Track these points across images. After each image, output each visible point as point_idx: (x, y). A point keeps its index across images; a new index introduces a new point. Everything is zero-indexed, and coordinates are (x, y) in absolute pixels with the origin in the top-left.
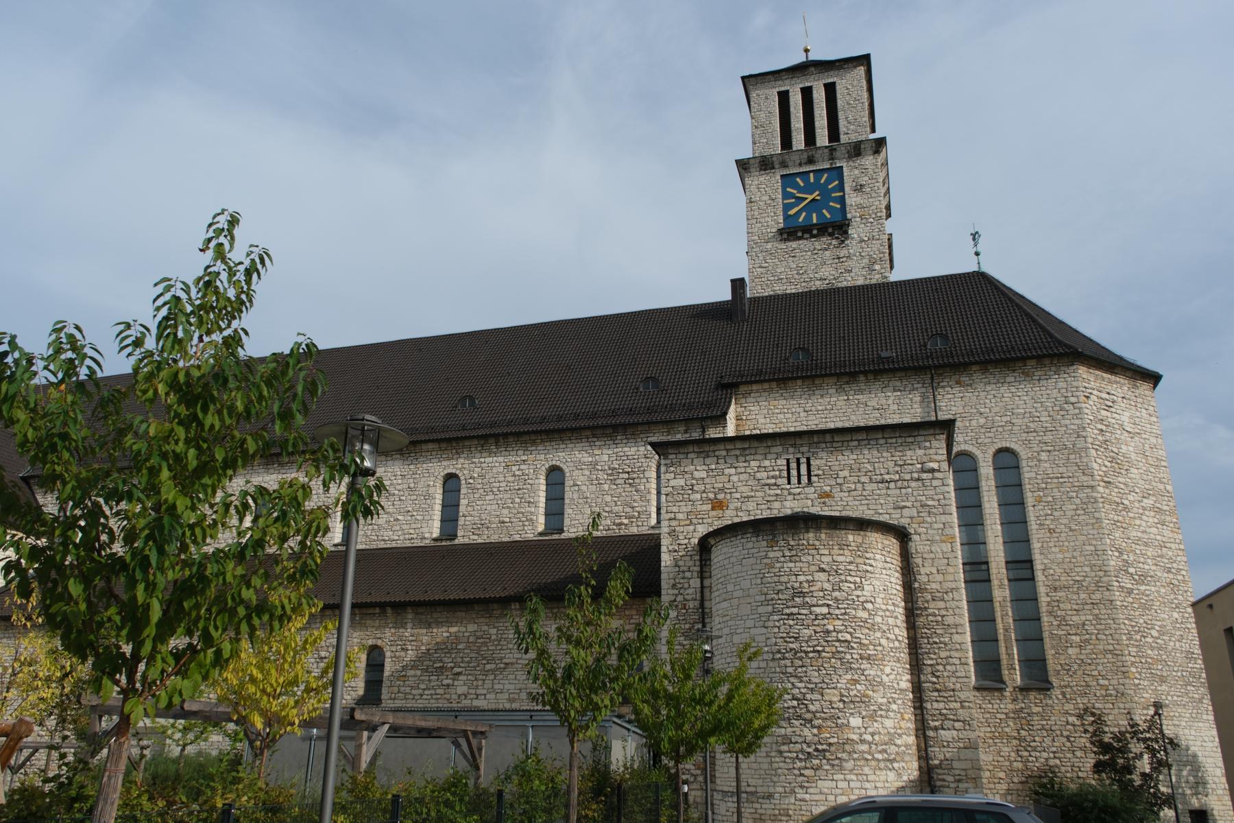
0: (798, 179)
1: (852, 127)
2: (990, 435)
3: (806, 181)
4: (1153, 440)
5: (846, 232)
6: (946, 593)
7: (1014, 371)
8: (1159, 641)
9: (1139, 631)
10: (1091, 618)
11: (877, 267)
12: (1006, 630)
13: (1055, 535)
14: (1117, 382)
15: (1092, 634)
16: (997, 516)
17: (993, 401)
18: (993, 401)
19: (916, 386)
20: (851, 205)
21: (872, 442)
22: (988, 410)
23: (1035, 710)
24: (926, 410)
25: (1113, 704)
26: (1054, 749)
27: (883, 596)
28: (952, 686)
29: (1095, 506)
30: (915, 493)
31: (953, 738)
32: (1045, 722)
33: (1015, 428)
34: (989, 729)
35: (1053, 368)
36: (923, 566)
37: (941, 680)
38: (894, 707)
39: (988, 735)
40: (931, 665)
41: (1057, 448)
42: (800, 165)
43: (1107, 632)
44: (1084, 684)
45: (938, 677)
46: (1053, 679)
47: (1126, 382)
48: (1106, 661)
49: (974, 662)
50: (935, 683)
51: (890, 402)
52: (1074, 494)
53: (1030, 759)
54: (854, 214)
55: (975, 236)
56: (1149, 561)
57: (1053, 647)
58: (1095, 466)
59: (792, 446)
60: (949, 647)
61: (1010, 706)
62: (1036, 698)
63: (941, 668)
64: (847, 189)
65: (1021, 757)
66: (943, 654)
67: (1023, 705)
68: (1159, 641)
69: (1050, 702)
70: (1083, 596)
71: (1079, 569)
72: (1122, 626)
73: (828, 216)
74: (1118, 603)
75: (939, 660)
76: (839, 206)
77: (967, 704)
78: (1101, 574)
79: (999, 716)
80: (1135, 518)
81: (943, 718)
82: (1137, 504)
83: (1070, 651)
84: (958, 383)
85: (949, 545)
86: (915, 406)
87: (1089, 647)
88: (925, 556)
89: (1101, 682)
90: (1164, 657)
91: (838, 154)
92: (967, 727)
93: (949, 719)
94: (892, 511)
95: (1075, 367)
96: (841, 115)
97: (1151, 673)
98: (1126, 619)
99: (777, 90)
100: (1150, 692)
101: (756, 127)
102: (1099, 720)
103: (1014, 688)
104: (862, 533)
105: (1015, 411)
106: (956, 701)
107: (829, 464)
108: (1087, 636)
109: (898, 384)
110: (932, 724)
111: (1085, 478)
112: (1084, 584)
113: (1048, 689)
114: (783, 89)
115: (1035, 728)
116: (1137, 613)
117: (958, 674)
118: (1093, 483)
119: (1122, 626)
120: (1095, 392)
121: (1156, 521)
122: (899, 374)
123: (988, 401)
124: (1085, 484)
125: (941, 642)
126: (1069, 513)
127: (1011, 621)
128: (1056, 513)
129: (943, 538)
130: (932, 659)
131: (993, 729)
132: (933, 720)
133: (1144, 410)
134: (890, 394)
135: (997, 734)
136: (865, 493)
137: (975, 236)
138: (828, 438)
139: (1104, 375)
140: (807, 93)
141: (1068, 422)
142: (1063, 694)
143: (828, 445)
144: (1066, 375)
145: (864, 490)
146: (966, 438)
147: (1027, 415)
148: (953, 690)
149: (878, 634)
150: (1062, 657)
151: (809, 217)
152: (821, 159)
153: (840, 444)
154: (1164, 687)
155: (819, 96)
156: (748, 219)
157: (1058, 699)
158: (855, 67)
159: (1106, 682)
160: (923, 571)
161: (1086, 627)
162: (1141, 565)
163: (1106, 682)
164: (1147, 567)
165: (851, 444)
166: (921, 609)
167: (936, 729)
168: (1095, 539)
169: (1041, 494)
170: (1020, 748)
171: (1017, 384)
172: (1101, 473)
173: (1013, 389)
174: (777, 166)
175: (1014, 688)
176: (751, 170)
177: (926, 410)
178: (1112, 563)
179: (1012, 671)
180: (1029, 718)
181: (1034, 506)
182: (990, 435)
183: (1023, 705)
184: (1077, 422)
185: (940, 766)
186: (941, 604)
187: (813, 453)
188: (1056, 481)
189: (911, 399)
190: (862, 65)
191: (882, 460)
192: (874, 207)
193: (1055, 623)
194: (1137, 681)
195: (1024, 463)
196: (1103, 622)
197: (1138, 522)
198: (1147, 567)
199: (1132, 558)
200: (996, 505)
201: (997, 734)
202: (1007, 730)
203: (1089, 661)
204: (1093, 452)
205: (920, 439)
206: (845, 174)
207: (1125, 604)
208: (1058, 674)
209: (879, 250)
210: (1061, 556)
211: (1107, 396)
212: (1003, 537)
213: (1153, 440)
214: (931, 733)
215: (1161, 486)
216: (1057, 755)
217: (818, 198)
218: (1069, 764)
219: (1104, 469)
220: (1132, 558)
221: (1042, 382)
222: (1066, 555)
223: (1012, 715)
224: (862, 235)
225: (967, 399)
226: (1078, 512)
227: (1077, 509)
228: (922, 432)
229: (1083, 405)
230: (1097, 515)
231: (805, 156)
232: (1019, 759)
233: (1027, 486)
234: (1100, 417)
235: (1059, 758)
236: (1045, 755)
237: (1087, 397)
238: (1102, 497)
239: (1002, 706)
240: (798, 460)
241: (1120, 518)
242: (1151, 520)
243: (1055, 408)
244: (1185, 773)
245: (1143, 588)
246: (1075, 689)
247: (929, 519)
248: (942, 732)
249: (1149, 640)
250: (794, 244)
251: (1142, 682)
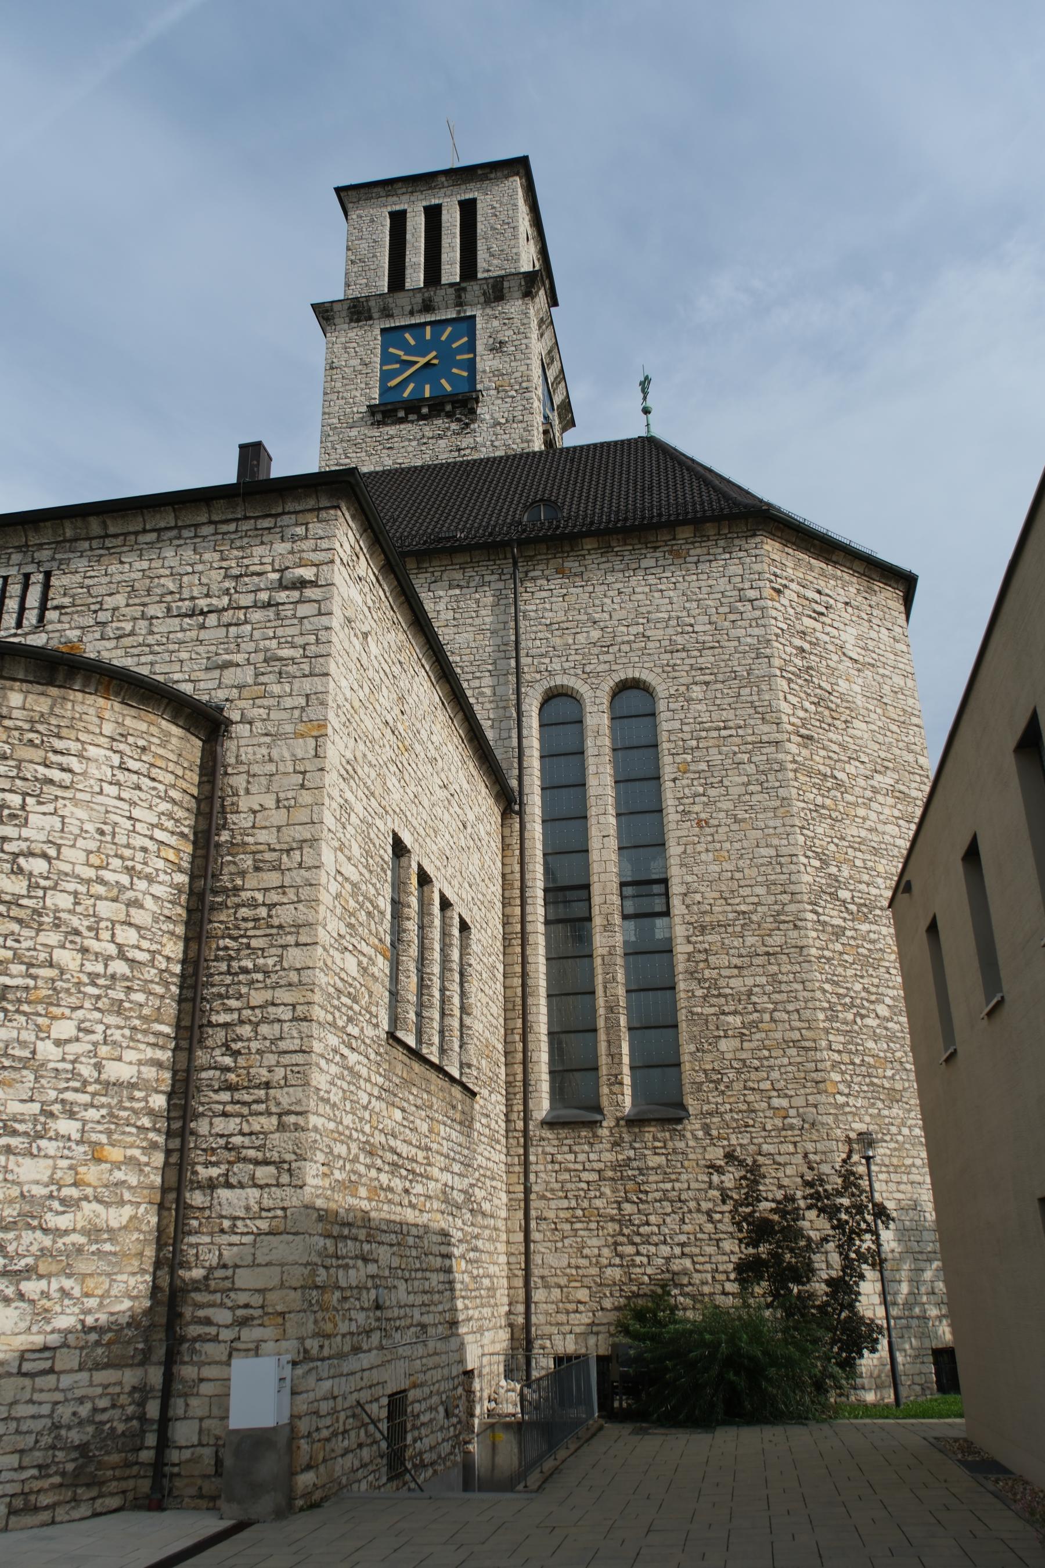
0: (407, 336)
1: (495, 262)
2: (609, 657)
3: (420, 338)
4: (898, 680)
5: (473, 411)
6: (288, 851)
7: (655, 548)
8: (890, 1025)
9: (852, 1006)
10: (763, 980)
12: (610, 1009)
13: (708, 830)
14: (836, 578)
15: (763, 1011)
16: (611, 800)
17: (617, 600)
18: (617, 600)
19: (487, 578)
20: (484, 372)
21: (186, 533)
22: (606, 616)
23: (653, 1161)
24: (502, 618)
25: (795, 1143)
26: (683, 1238)
27: (93, 845)
28: (264, 1074)
29: (780, 776)
30: (257, 634)
31: (248, 1208)
32: (668, 1186)
33: (650, 645)
34: (565, 1204)
35: (722, 543)
36: (248, 792)
37: (241, 1061)
38: (66, 1126)
39: (563, 1214)
40: (226, 1025)
41: (720, 677)
42: (412, 313)
43: (790, 1007)
44: (745, 1107)
45: (236, 1054)
46: (690, 1101)
47: (854, 580)
48: (786, 1061)
49: (551, 1072)
50: (227, 1069)
51: (441, 606)
52: (746, 757)
53: (638, 1259)
54: (487, 383)
55: (645, 384)
56: (880, 881)
57: (693, 1038)
58: (785, 707)
59: (19, 548)
60: (274, 977)
61: (608, 1156)
62: (655, 1139)
63: (246, 1031)
64: (480, 348)
65: (621, 1256)
66: (258, 997)
67: (631, 1153)
68: (890, 1025)
69: (681, 1145)
70: (750, 940)
71: (747, 891)
72: (818, 994)
73: (449, 388)
74: (813, 951)
75: (247, 1013)
76: (465, 374)
77: (292, 1119)
78: (786, 898)
79: (585, 1176)
80: (856, 805)
81: (231, 1156)
82: (861, 782)
83: (724, 1045)
84: (560, 571)
85: (311, 742)
86: (483, 612)
87: (758, 1036)
88: (255, 769)
89: (776, 1102)
90: (898, 1054)
91: (468, 297)
92: (285, 1179)
93: (246, 1160)
94: (202, 675)
95: (758, 539)
96: (481, 245)
97: (872, 1084)
98: (827, 981)
99: (389, 209)
100: (867, 1119)
101: (353, 262)
102: (753, 1175)
103: (618, 1120)
104: (54, 691)
105: (653, 616)
106: (270, 1114)
107: (88, 582)
108: (756, 1015)
109: (458, 575)
110: (204, 1173)
111: (766, 728)
112: (754, 918)
113: (679, 1121)
114: (397, 208)
115: (650, 1197)
116: (850, 972)
117: (283, 1045)
118: (779, 737)
119: (818, 994)
120: (794, 586)
121: (897, 813)
122: (459, 559)
123: (608, 601)
124: (765, 738)
125: (257, 969)
126: (735, 791)
127: (621, 991)
128: (711, 792)
129: (301, 727)
130: (231, 1010)
131: (573, 1204)
132: (207, 1164)
133: (883, 630)
134: (441, 593)
135: (579, 1213)
136: (151, 640)
137: (645, 384)
138: (95, 526)
139: (813, 561)
140: (433, 215)
141: (741, 632)
142: (706, 1128)
143: (95, 544)
144: (742, 554)
145: (151, 633)
146: (566, 665)
147: (673, 623)
148: (267, 1085)
149: (52, 938)
150: (708, 1057)
151: (419, 388)
152: (442, 305)
153: (119, 541)
154: (895, 1111)
155: (451, 219)
156: (325, 394)
157: (695, 1137)
158: (507, 177)
159: (784, 1103)
160: (244, 804)
161: (754, 999)
162: (863, 887)
163: (784, 1103)
164: (874, 891)
165: (141, 538)
166: (225, 890)
167: (211, 1185)
168: (778, 836)
169: (689, 758)
170: (621, 1239)
171: (659, 570)
172: (793, 720)
173: (651, 579)
174: (376, 315)
175: (618, 1120)
176: (337, 321)
177: (502, 618)
178: (807, 878)
179: (616, 1088)
180: (640, 1179)
181: (674, 780)
182: (609, 657)
183: (631, 1153)
184: (756, 631)
185: (203, 1285)
186: (272, 879)
187: (61, 562)
188: (715, 734)
189: (478, 601)
190: (517, 174)
191: (199, 568)
192: (518, 374)
193: (699, 993)
194: (841, 1099)
195: (662, 705)
196: (784, 987)
197: (861, 812)
198: (874, 891)
199: (846, 874)
200: (609, 780)
201: (579, 1213)
202: (598, 1203)
203: (756, 1063)
204: (784, 683)
205: (286, 520)
206: (478, 326)
207: (827, 953)
208: (699, 1090)
209: (521, 438)
210: (717, 869)
211: (817, 597)
212: (619, 838)
213: (898, 680)
214: (197, 1198)
215: (910, 758)
216: (687, 1250)
217: (435, 361)
218: (708, 1267)
219: (801, 714)
220: (846, 874)
221: (701, 566)
222: (726, 866)
223: (610, 1174)
224: (496, 415)
225: (573, 599)
226: (751, 788)
227: (749, 783)
228: (290, 507)
229: (770, 603)
230: (782, 792)
231: (418, 299)
232: (617, 1261)
233: (665, 745)
234: (799, 628)
235: (691, 1256)
236: (665, 1250)
237: (779, 592)
238: (794, 761)
239: (592, 1156)
240: (27, 576)
241: (828, 802)
242: (887, 811)
243: (721, 610)
244: (928, 1275)
245: (865, 927)
246: (727, 1117)
247: (276, 689)
248: (223, 1193)
249: (871, 1022)
250: (392, 430)
251: (851, 1101)
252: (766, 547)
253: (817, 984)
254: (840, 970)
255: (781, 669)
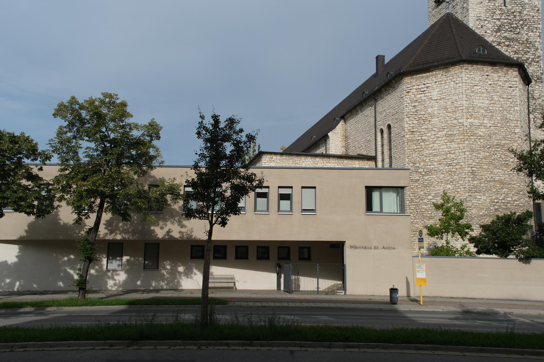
9: (419, 198)
11: (465, 5)
95: (403, 79)
97: (423, 216)
98: (411, 193)
116: (419, 190)
121: (446, 141)
139: (423, 75)
211: (423, 86)
245: (426, 177)
250: (440, 7)
252: (405, 81)
253: (408, 195)
254: (416, 190)
255: (406, 115)
